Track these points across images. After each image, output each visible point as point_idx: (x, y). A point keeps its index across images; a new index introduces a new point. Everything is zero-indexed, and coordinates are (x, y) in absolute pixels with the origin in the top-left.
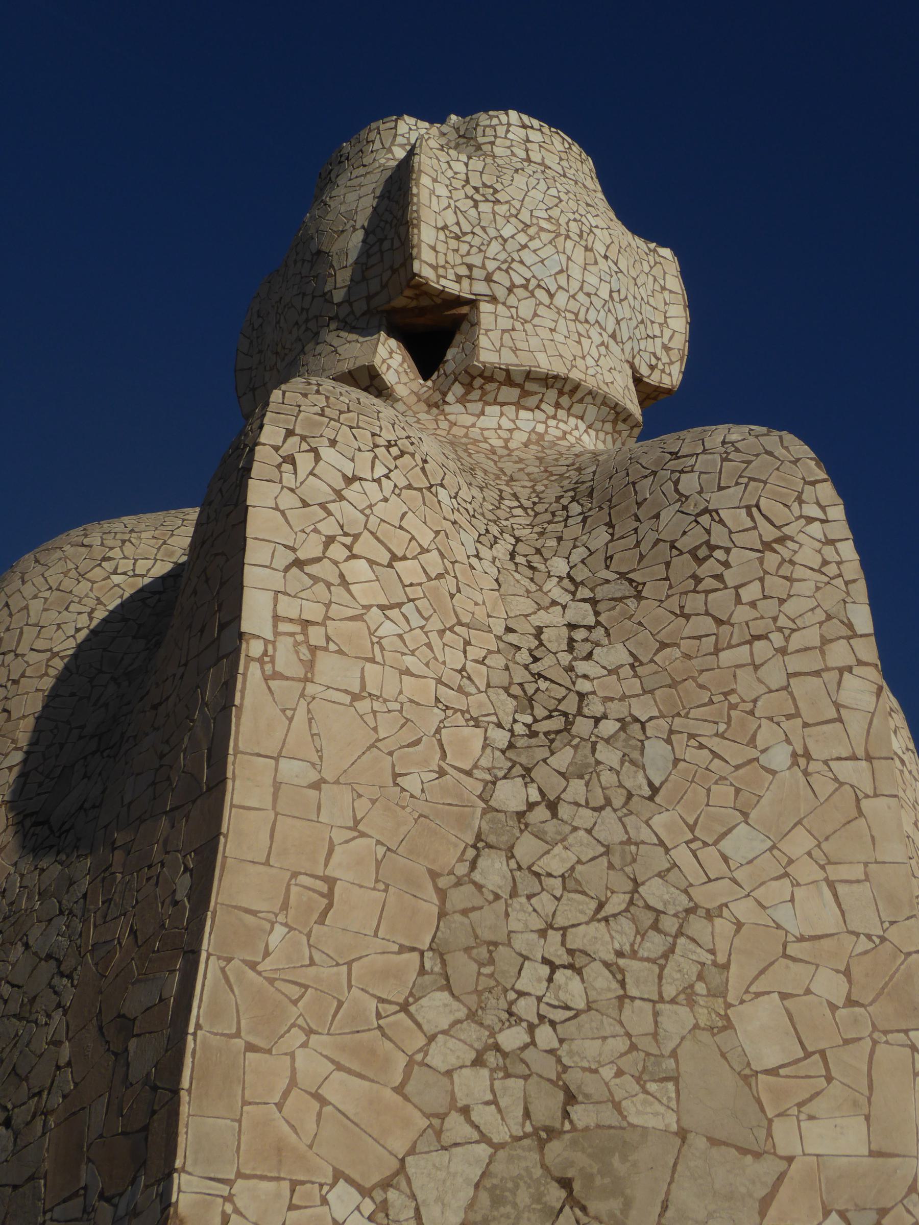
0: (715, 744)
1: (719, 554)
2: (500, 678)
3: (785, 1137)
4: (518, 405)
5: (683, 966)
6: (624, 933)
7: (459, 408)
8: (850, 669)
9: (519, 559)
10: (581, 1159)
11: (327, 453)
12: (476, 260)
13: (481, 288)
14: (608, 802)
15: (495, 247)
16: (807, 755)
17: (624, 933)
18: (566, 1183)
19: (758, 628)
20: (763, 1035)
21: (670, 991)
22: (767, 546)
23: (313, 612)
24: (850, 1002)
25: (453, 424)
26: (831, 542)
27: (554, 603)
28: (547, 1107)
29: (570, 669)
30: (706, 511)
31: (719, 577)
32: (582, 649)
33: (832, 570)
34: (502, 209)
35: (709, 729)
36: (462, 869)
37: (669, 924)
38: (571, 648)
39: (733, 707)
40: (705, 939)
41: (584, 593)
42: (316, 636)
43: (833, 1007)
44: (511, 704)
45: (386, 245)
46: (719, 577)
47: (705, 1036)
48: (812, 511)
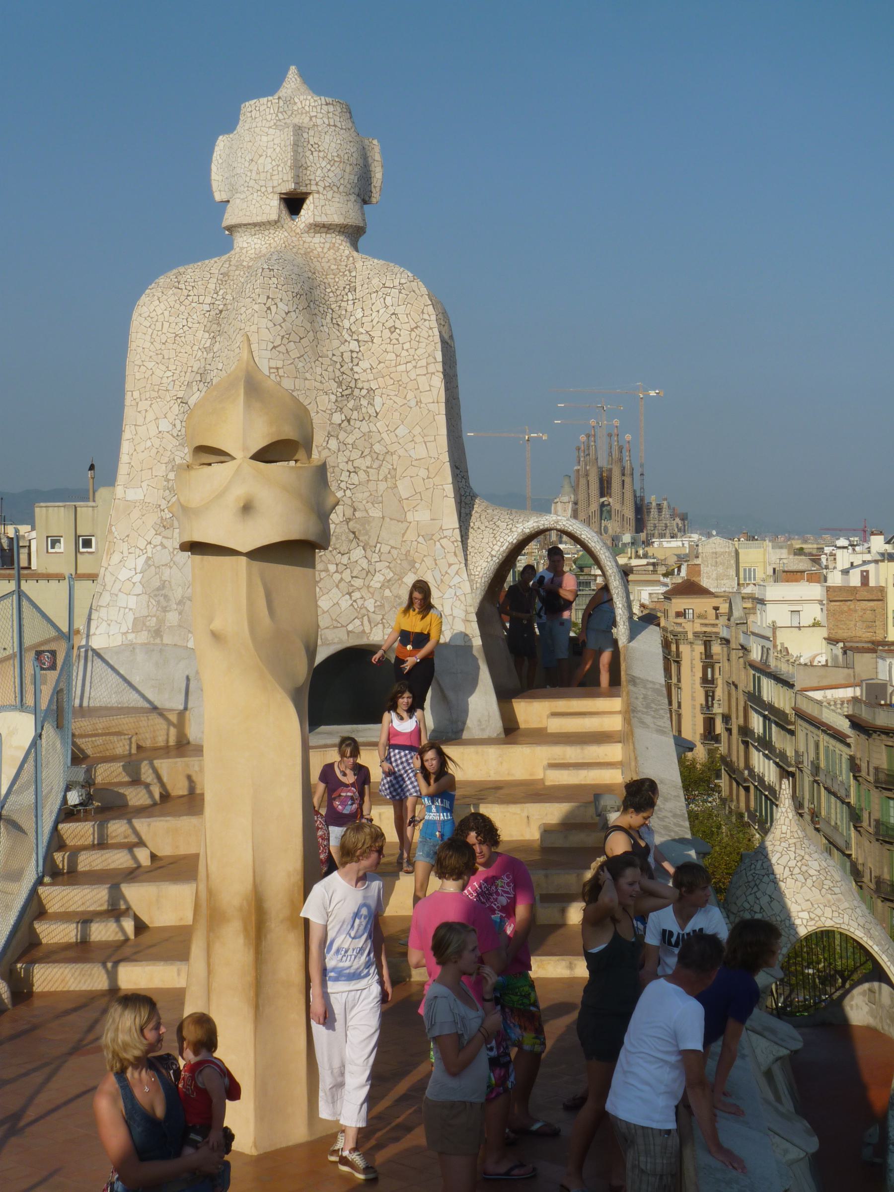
0: (393, 398)
1: (397, 331)
2: (332, 376)
3: (410, 517)
4: (326, 233)
5: (384, 470)
6: (368, 461)
7: (306, 235)
8: (434, 373)
9: (334, 321)
10: (358, 526)
11: (280, 305)
12: (312, 177)
13: (314, 188)
14: (364, 419)
15: (319, 171)
16: (421, 402)
17: (368, 461)
18: (354, 533)
19: (409, 358)
20: (404, 490)
21: (381, 478)
22: (412, 330)
23: (280, 364)
24: (428, 478)
25: (304, 242)
26: (431, 328)
27: (346, 341)
28: (349, 512)
29: (352, 369)
30: (393, 314)
31: (397, 340)
32: (355, 361)
33: (431, 339)
34: (321, 154)
35: (394, 393)
36: (325, 444)
37: (381, 457)
38: (352, 362)
39: (400, 386)
40: (391, 461)
41: (355, 337)
42: (281, 372)
43: (424, 479)
44: (336, 385)
45: (280, 169)
46: (397, 340)
47: (389, 490)
48: (426, 316)
